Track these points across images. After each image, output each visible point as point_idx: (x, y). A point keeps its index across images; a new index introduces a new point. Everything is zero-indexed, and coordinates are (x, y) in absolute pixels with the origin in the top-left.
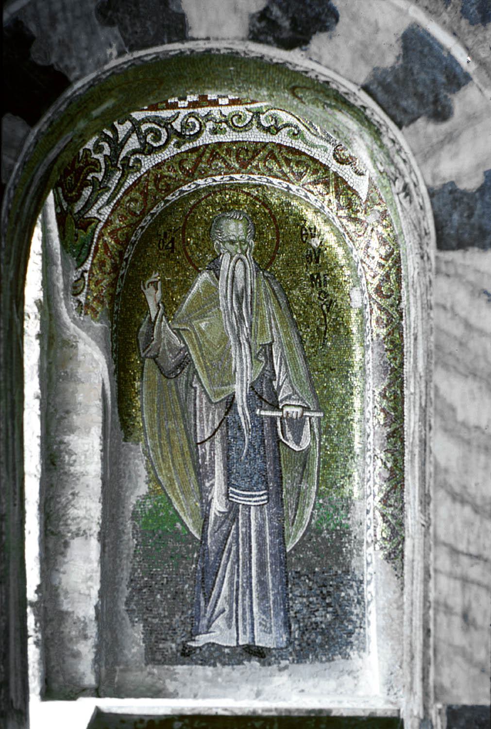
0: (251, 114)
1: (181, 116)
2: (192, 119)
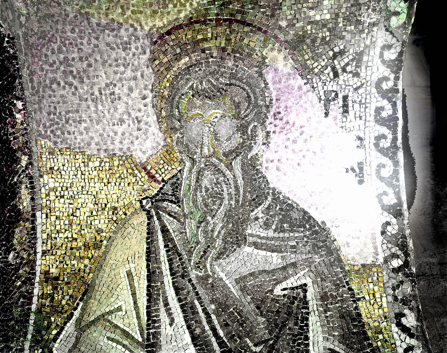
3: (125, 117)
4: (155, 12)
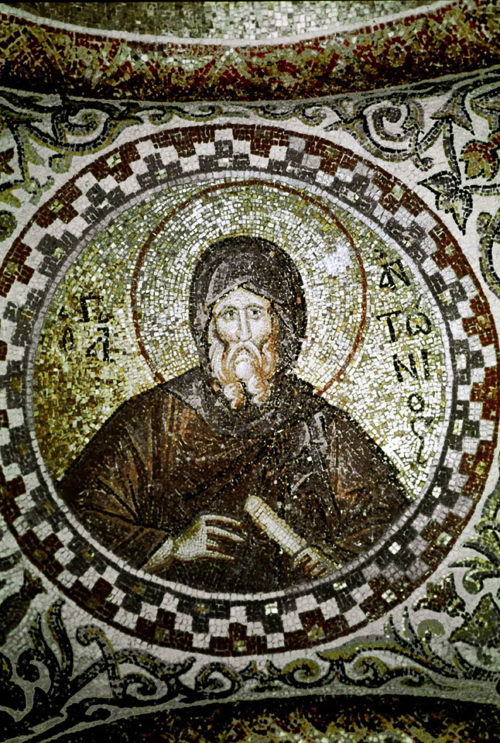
0: (327, 664)
1: (196, 667)
2: (216, 675)
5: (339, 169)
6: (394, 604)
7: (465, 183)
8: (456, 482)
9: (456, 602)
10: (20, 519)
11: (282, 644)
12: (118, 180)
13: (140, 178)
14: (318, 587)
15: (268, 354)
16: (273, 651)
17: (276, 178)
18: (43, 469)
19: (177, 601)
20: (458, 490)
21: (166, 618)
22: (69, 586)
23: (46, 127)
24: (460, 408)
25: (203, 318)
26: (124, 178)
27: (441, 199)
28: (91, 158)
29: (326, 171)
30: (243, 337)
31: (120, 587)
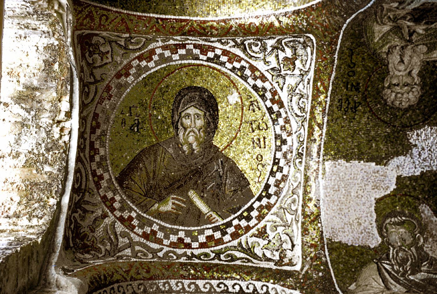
0: (214, 254)
2: (171, 254)
3: (363, 231)
4: (376, 192)
5: (235, 62)
6: (242, 235)
7: (283, 73)
8: (272, 190)
9: (266, 235)
10: (101, 190)
11: (198, 246)
12: (148, 62)
13: (155, 62)
14: (215, 226)
15: (202, 134)
16: (194, 249)
17: (210, 64)
18: (111, 172)
19: (158, 227)
20: (272, 193)
21: (154, 233)
22: (118, 216)
23: (123, 43)
24: (277, 161)
25: (176, 118)
26: (149, 61)
27: (274, 77)
28: (137, 54)
29: (230, 63)
30: (193, 126)
31: (137, 219)
